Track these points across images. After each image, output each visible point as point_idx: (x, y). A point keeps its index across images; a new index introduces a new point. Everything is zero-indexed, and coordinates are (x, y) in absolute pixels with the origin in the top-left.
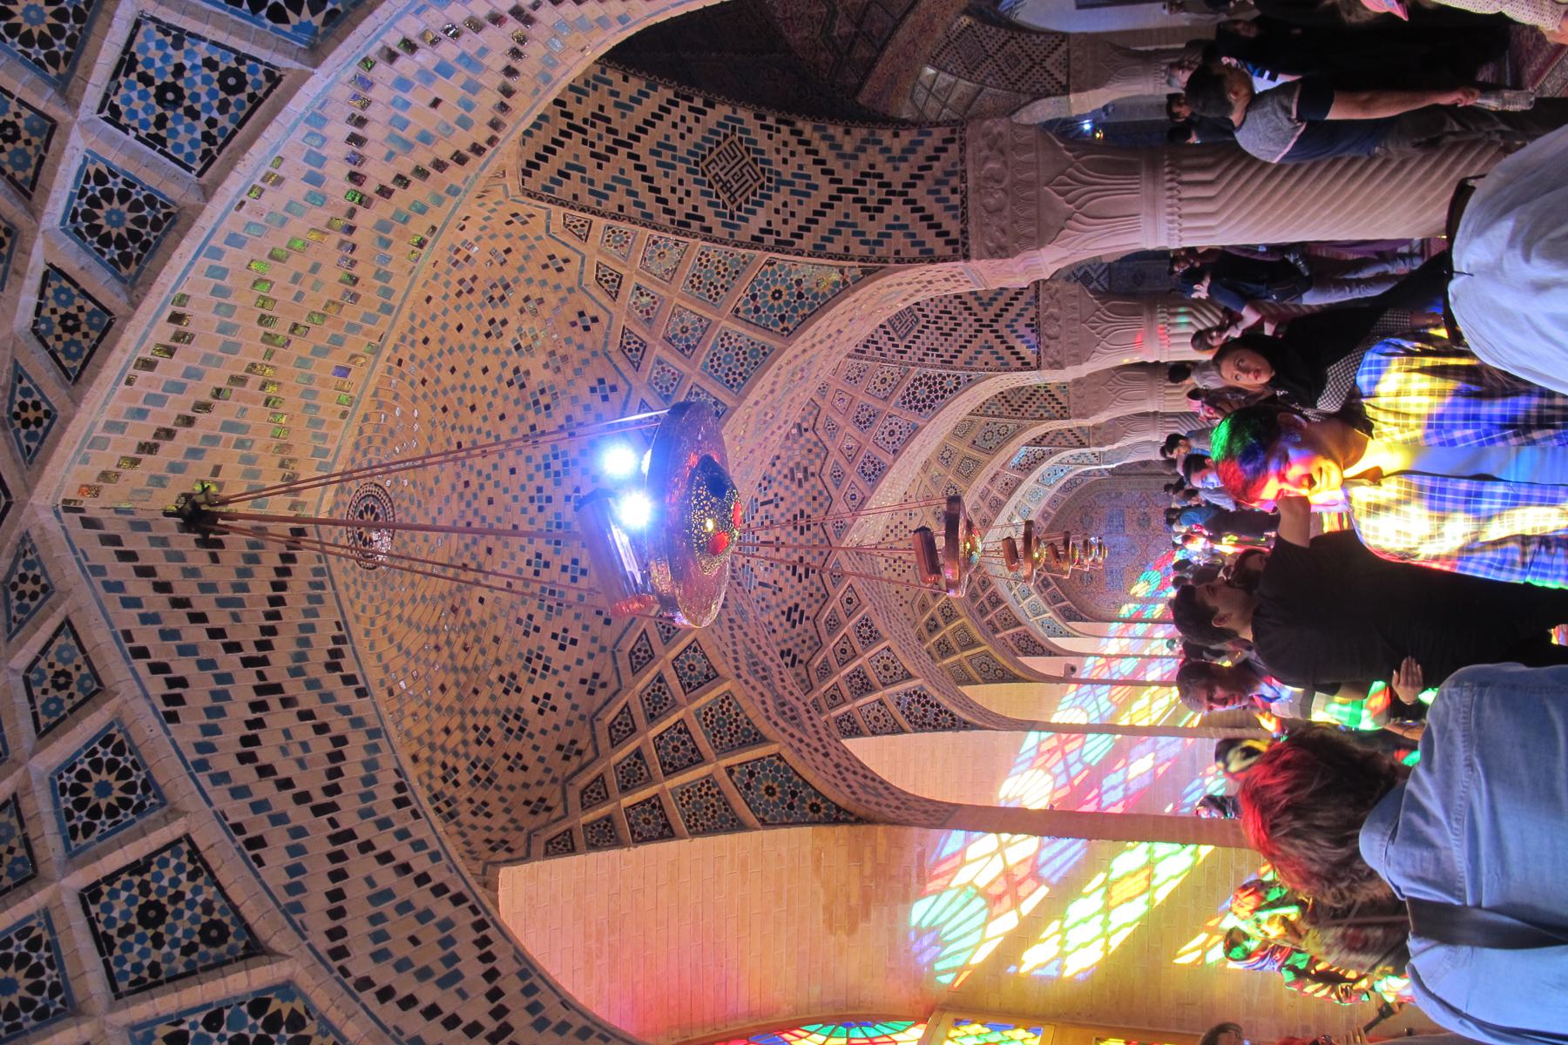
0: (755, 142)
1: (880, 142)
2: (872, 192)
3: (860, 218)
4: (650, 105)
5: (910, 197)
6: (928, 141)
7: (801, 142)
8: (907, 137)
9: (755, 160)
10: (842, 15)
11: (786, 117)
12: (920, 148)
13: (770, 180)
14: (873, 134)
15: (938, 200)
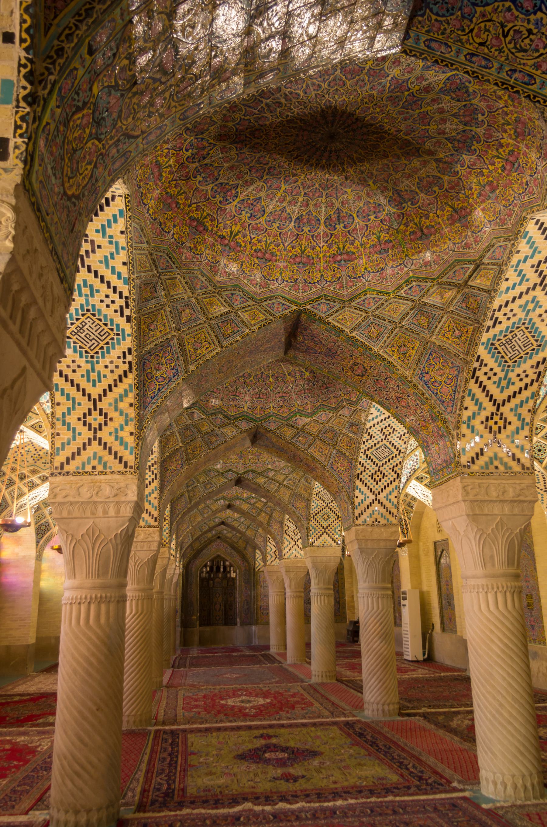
0: (114, 348)
1: (127, 424)
2: (95, 419)
3: (79, 412)
4: (114, 281)
5: (93, 442)
6: (127, 452)
7: (120, 376)
8: (131, 441)
9: (102, 348)
10: (307, 420)
11: (134, 368)
12: (123, 448)
13: (92, 357)
14: (131, 420)
15: (89, 458)
